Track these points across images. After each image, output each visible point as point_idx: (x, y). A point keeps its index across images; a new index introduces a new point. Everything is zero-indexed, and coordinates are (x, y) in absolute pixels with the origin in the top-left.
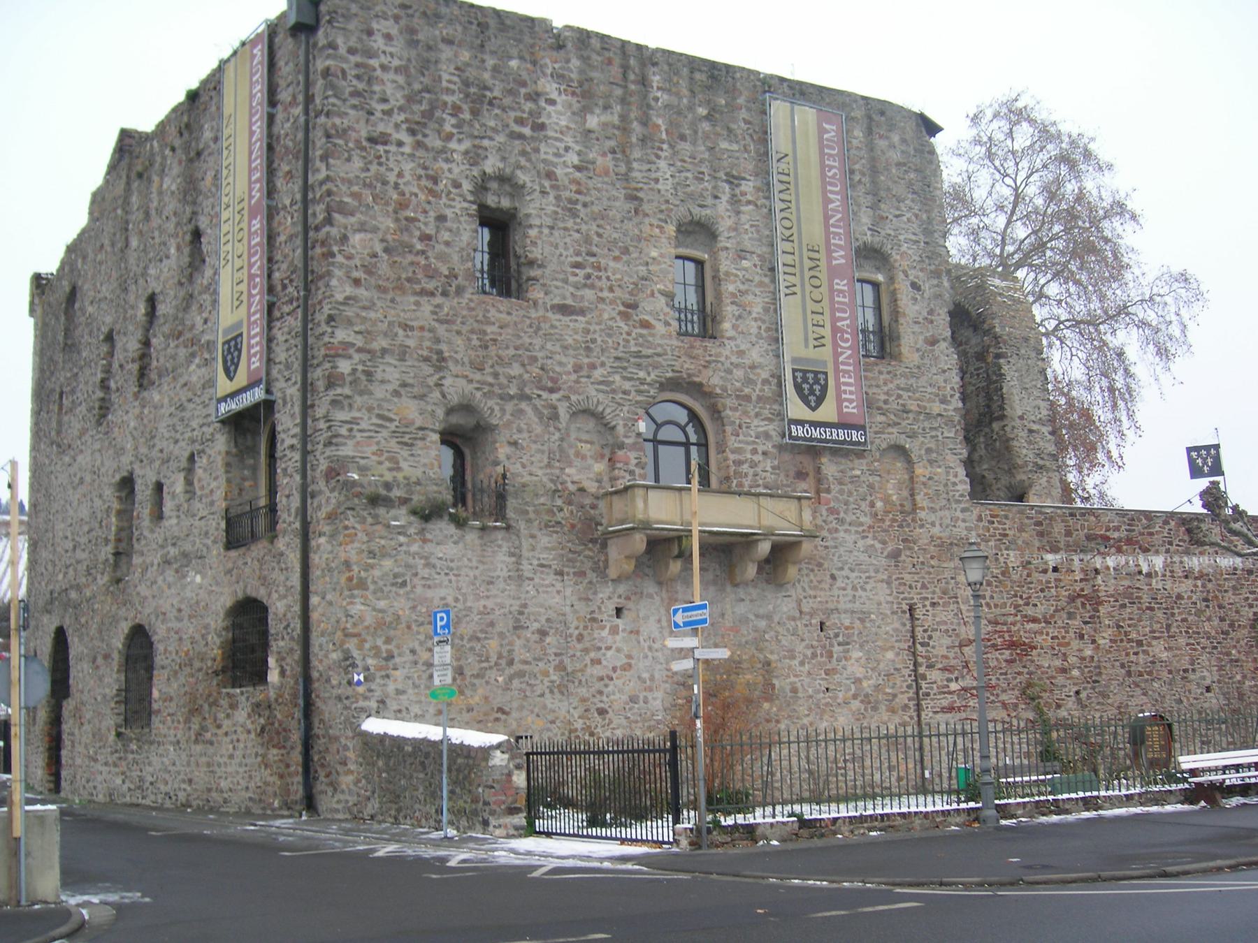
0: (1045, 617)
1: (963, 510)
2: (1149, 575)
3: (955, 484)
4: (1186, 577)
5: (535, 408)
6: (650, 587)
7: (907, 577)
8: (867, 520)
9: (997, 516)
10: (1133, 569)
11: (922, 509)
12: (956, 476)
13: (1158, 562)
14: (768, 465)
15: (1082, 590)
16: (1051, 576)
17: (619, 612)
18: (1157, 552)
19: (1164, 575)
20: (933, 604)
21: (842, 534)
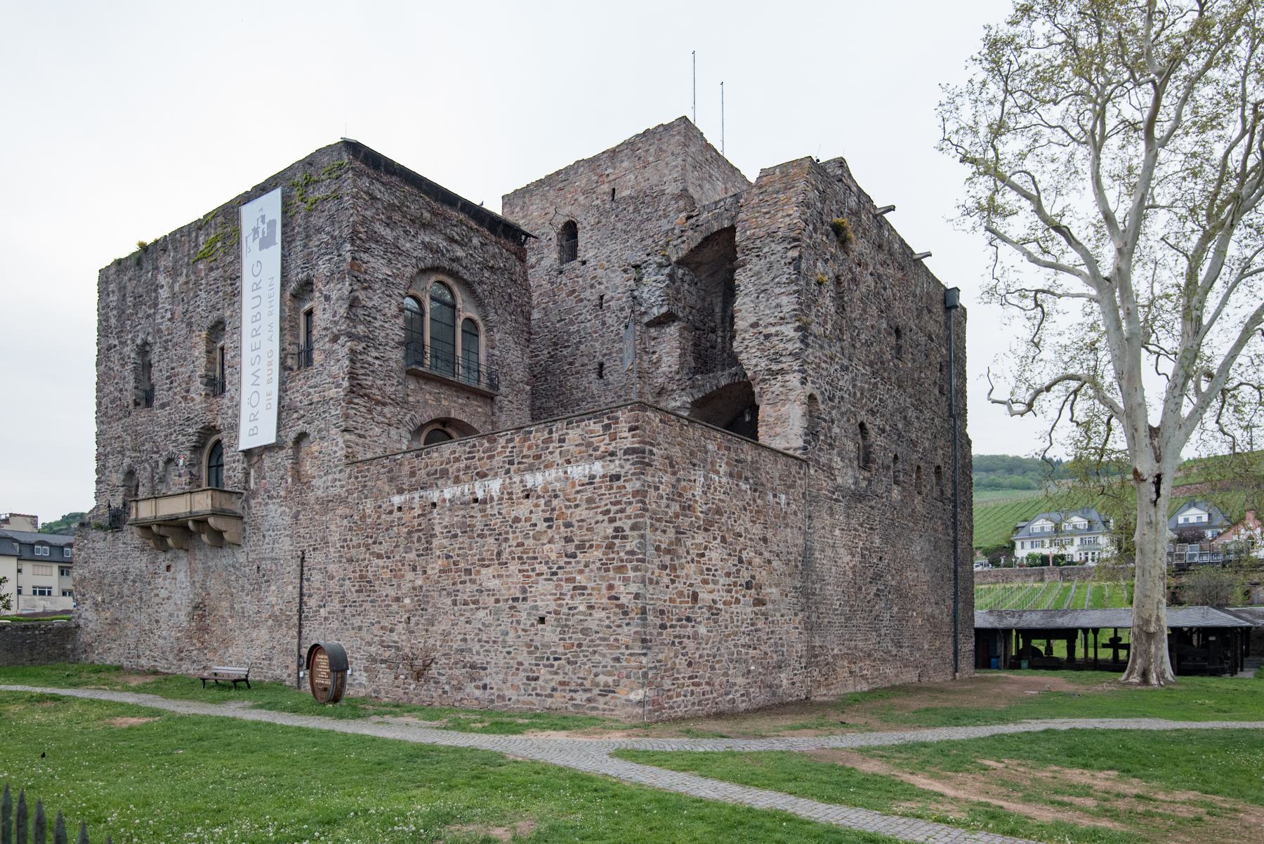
0: (386, 553)
1: (340, 471)
2: (484, 502)
3: (335, 452)
4: (527, 497)
5: (149, 464)
6: (182, 553)
7: (302, 530)
8: (283, 493)
9: (361, 471)
10: (468, 497)
11: (314, 477)
12: (337, 445)
13: (495, 486)
14: (240, 466)
15: (420, 525)
16: (397, 514)
17: (168, 568)
18: (496, 475)
19: (501, 499)
20: (314, 550)
21: (271, 506)
